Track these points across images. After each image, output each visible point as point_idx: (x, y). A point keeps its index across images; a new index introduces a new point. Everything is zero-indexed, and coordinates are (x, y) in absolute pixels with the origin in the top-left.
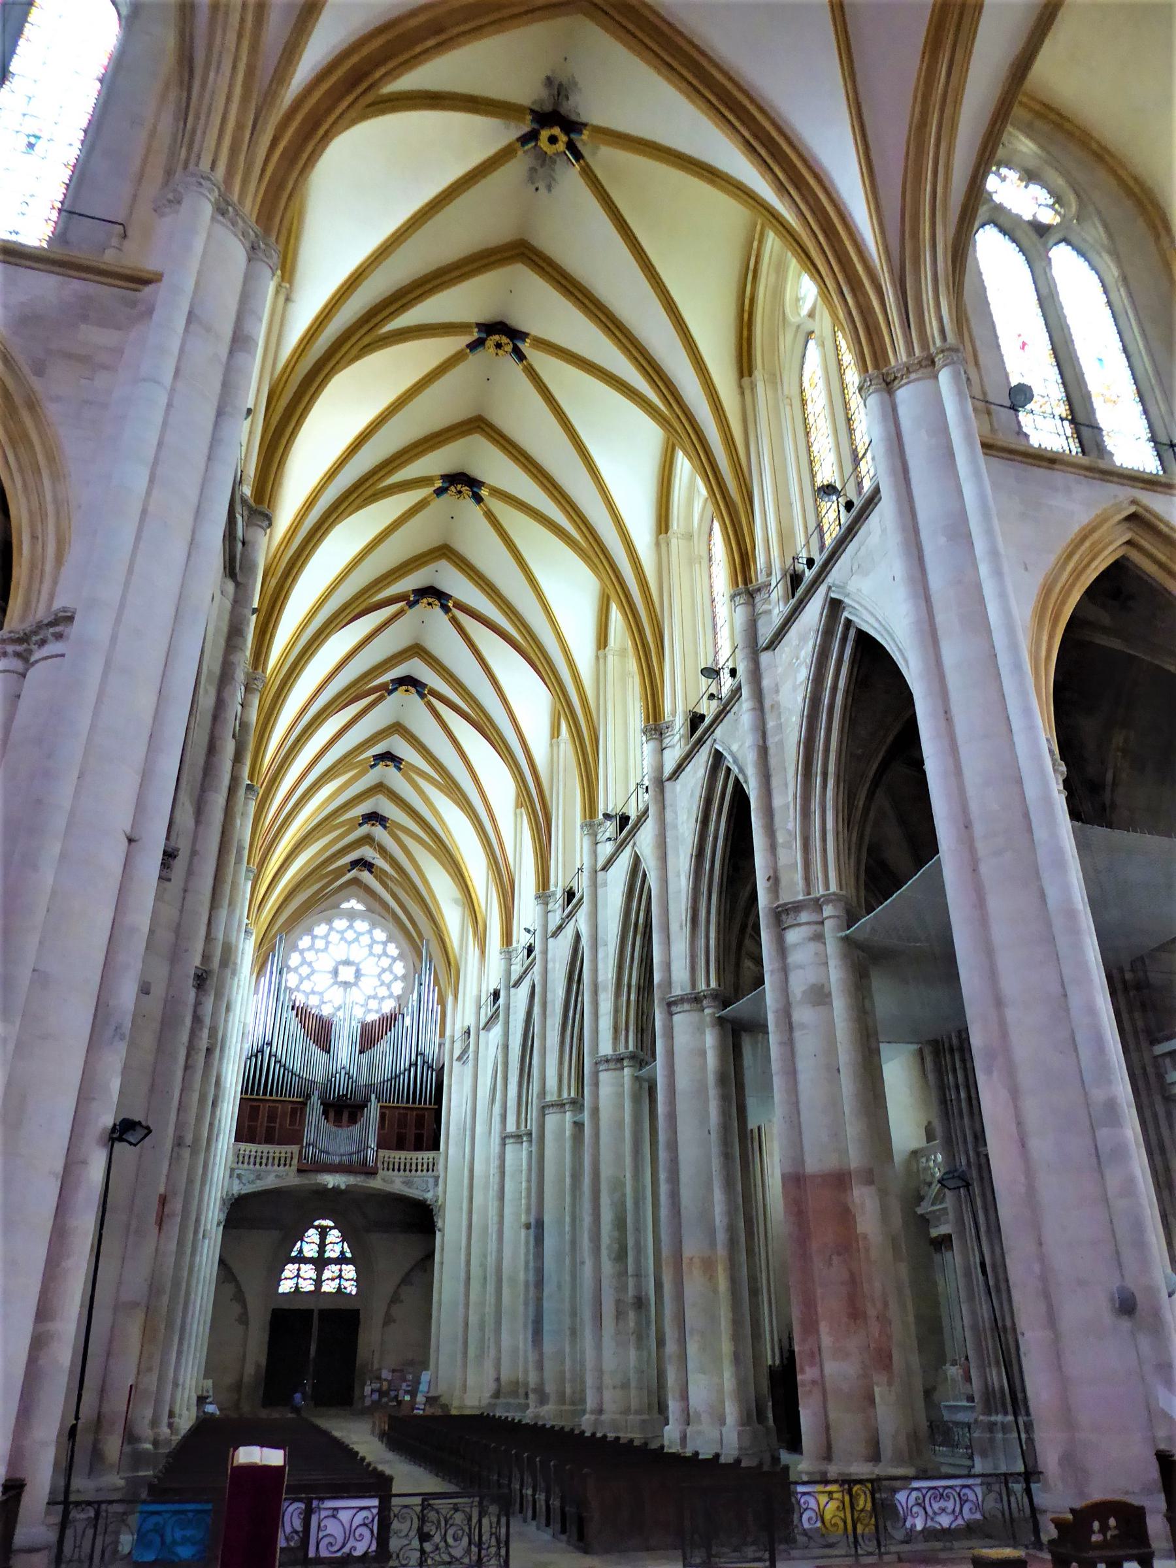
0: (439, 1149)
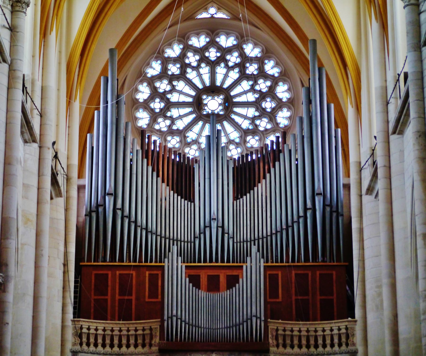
0: (353, 316)
